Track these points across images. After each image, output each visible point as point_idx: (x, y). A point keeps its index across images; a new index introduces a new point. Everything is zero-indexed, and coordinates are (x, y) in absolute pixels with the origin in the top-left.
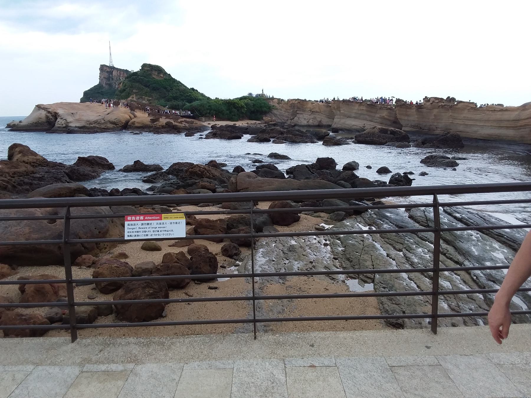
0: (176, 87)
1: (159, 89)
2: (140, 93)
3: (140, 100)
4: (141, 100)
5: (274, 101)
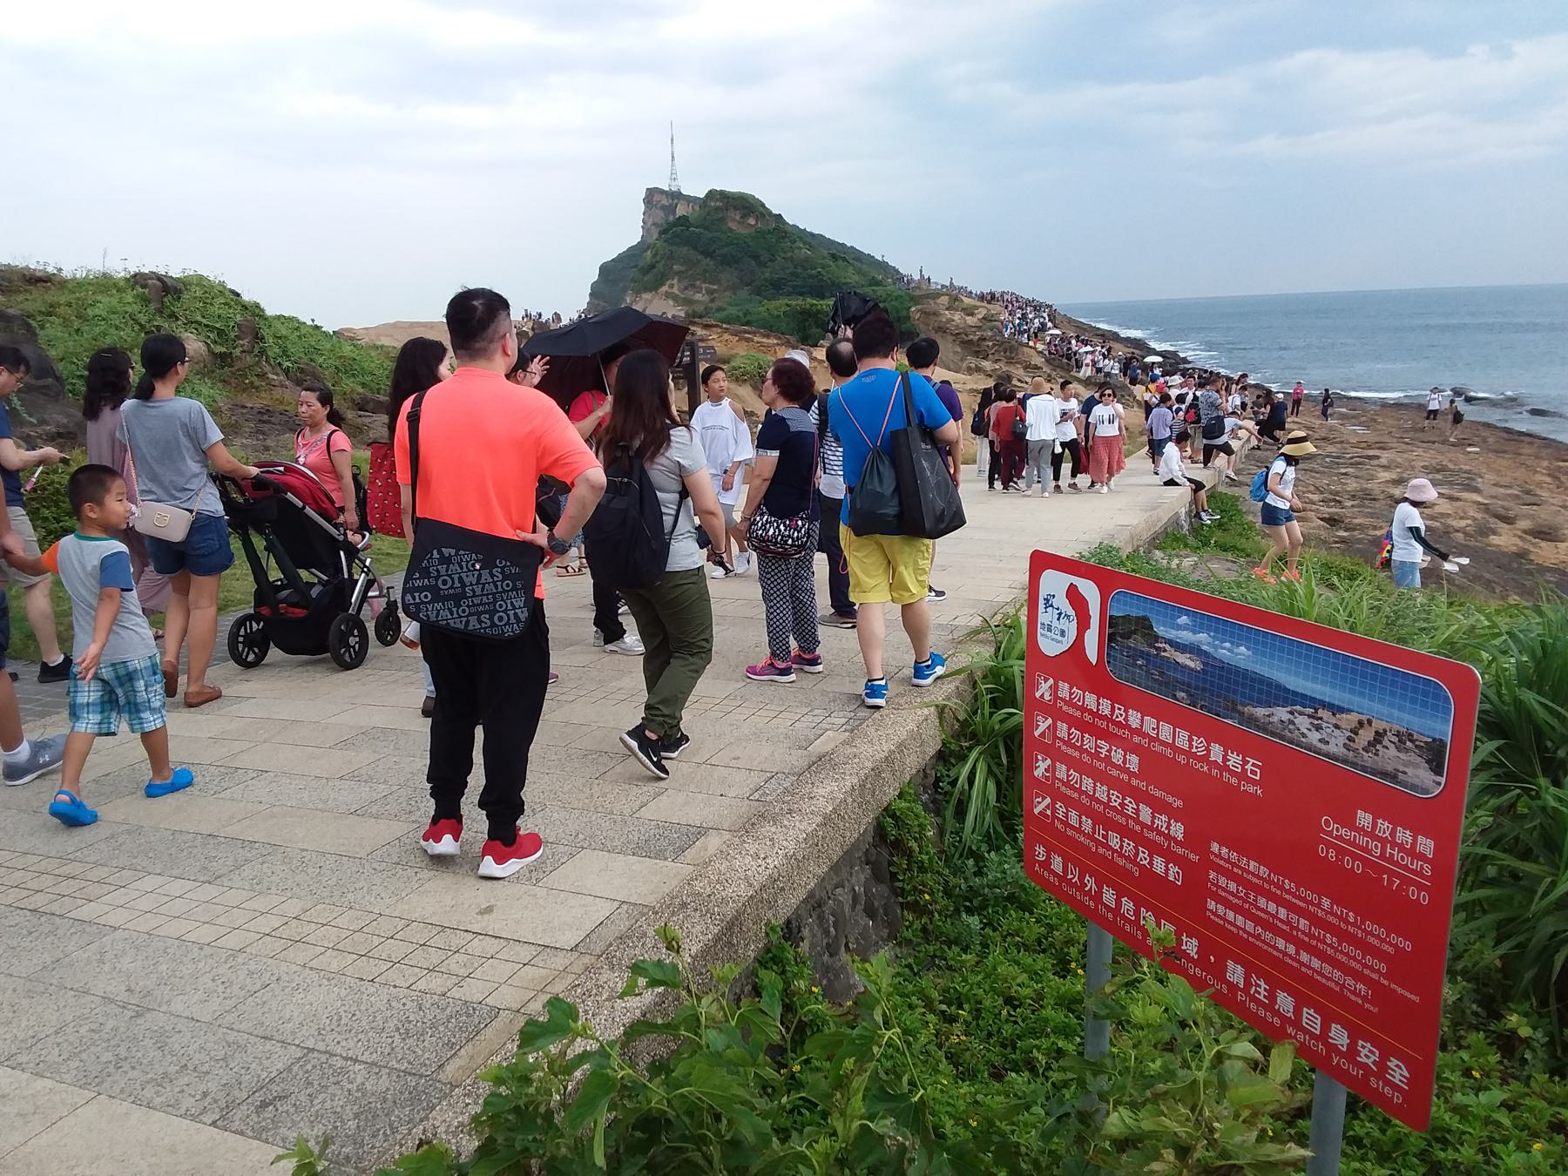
0: (785, 253)
2: (691, 272)
3: (689, 293)
5: (939, 301)
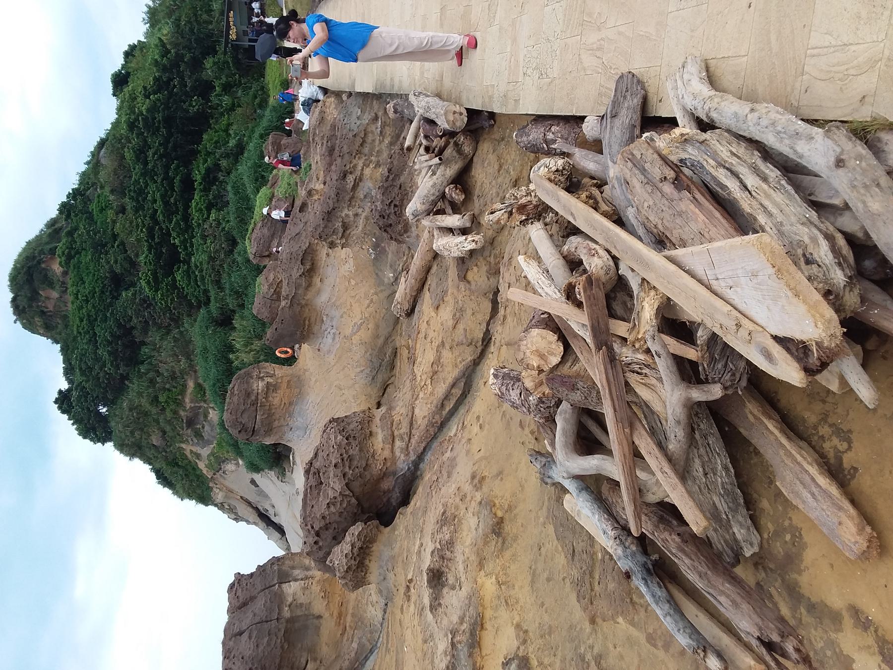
1: (120, 326)
4: (207, 428)
